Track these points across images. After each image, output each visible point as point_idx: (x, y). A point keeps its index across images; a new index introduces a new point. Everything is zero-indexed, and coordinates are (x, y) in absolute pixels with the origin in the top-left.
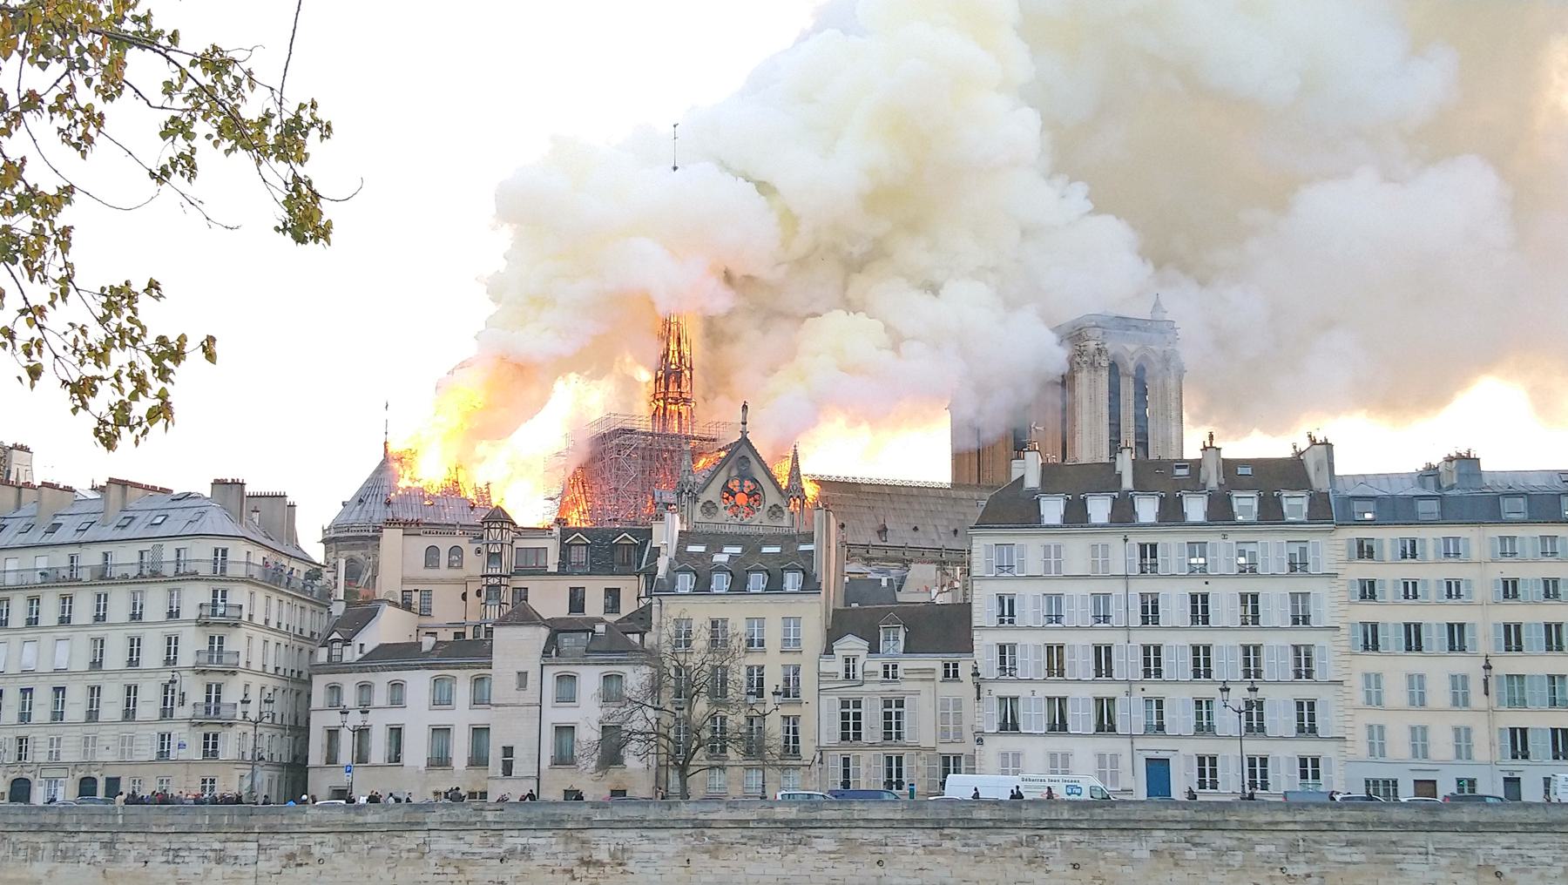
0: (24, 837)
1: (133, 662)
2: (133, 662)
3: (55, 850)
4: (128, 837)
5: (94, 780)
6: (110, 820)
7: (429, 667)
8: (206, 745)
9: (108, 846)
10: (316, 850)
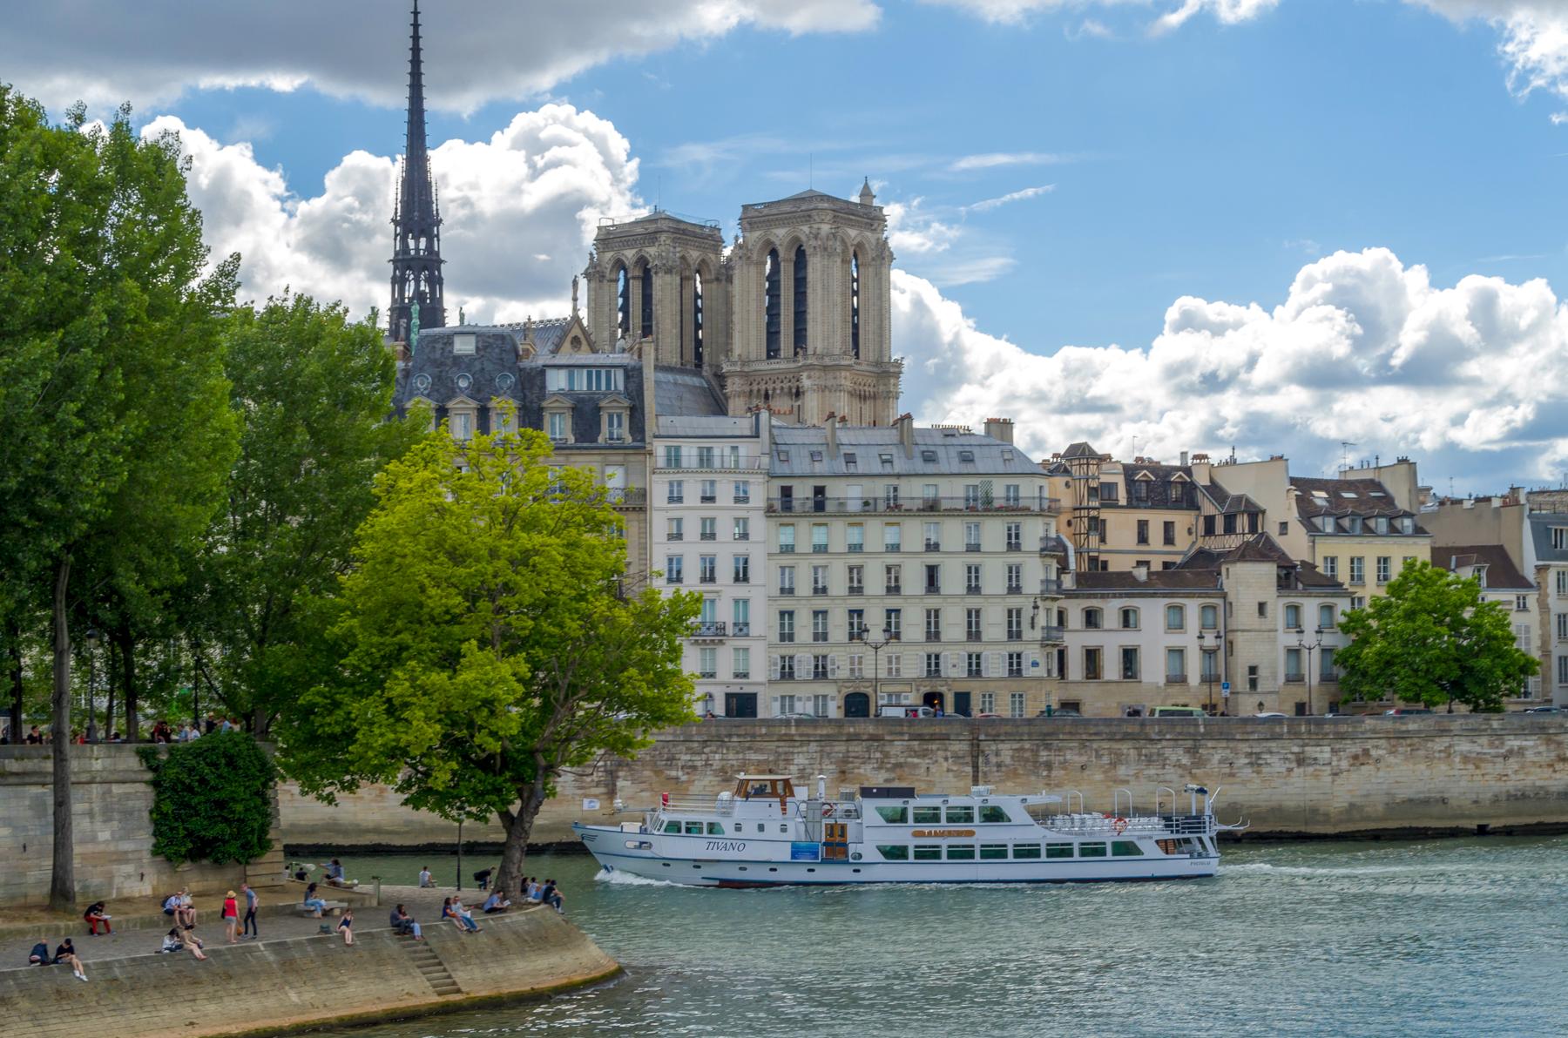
0: (1106, 745)
1: (974, 589)
2: (974, 589)
3: (1140, 755)
4: (1210, 744)
5: (940, 696)
6: (1192, 730)
7: (1165, 596)
8: (1011, 664)
9: (1193, 751)
10: (1373, 752)
